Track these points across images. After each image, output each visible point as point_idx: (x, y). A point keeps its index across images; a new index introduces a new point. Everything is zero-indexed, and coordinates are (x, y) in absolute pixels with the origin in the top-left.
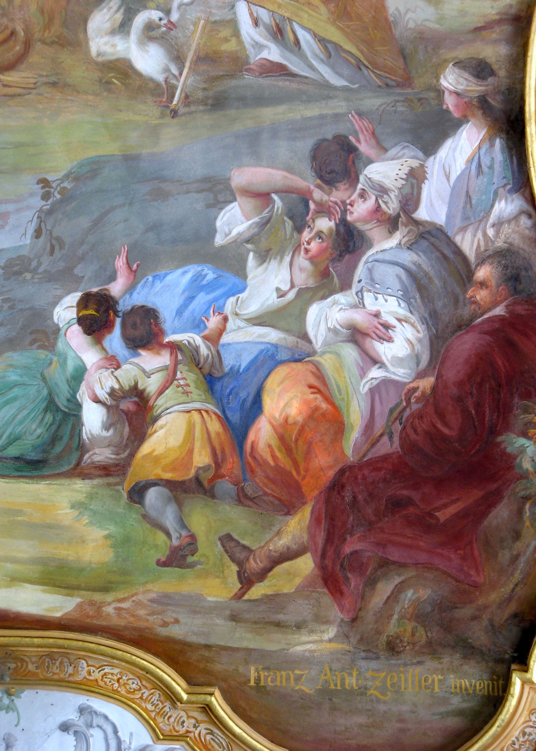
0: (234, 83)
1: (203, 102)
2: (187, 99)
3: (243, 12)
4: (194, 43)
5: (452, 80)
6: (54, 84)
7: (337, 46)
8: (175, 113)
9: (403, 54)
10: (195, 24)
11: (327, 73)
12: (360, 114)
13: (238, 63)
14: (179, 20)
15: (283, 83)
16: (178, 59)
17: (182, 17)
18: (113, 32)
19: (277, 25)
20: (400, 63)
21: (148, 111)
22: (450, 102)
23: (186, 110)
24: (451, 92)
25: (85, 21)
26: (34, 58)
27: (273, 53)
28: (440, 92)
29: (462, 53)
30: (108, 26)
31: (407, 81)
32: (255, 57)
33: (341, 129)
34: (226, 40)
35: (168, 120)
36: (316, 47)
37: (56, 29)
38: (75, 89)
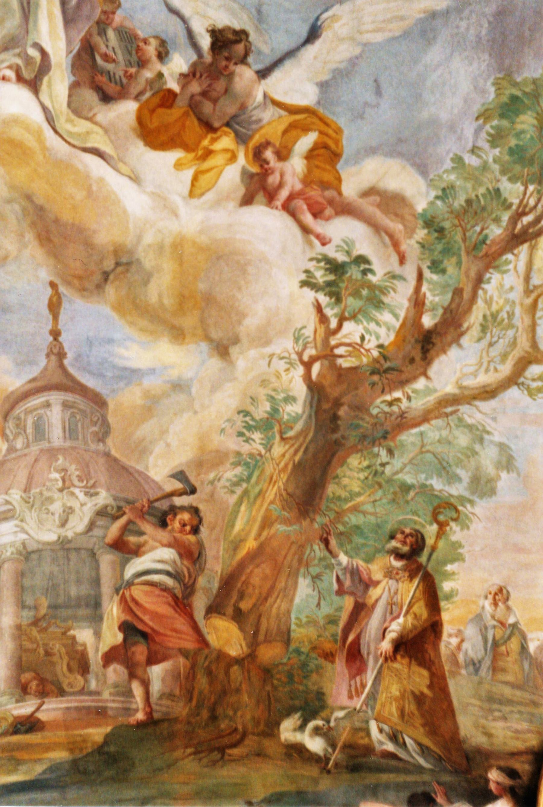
0: (364, 760)
1: (347, 767)
2: (336, 765)
3: (373, 726)
4: (343, 737)
5: (494, 775)
6: (258, 755)
7: (427, 748)
8: (329, 772)
9: (468, 758)
10: (344, 729)
11: (422, 761)
12: (439, 783)
13: (369, 750)
14: (335, 726)
15: (393, 763)
16: (333, 746)
17: (337, 725)
18: (295, 730)
19: (393, 734)
20: (464, 762)
21: (314, 771)
22: (492, 786)
23: (336, 771)
24: (493, 781)
25: (278, 724)
26: (247, 742)
27: (390, 747)
28: (487, 781)
29: (502, 763)
30: (292, 727)
31: (468, 771)
32: (378, 748)
33: (427, 789)
34: (362, 738)
35: (325, 775)
36: (415, 746)
37: (262, 727)
38: (270, 758)
